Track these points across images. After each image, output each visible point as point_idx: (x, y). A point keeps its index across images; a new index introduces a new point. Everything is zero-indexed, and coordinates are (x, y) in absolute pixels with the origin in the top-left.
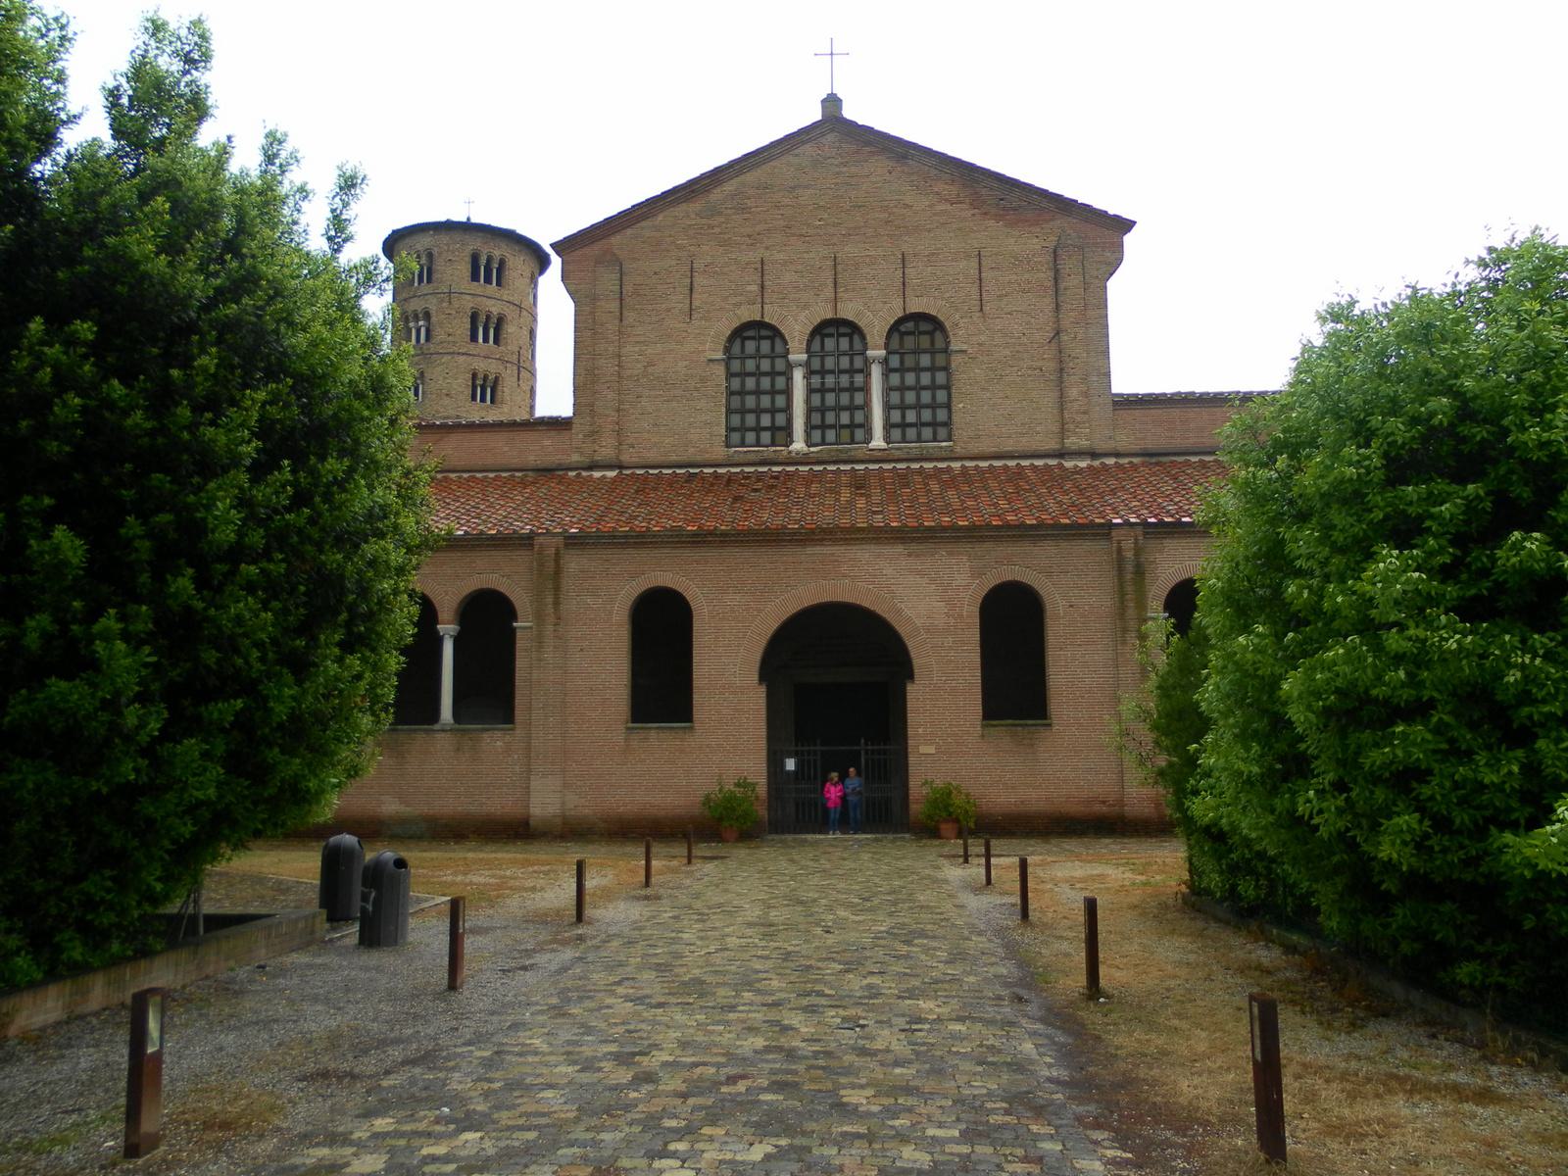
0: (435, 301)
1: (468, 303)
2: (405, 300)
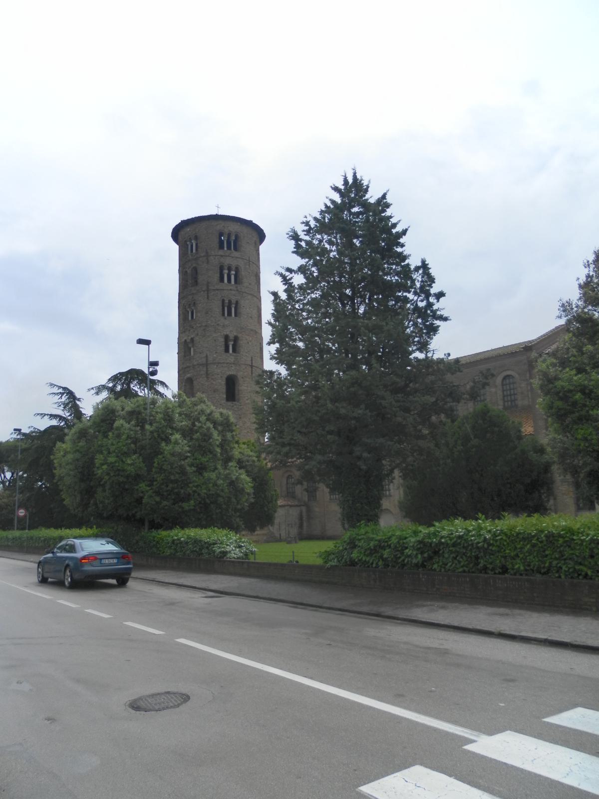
2: (222, 256)
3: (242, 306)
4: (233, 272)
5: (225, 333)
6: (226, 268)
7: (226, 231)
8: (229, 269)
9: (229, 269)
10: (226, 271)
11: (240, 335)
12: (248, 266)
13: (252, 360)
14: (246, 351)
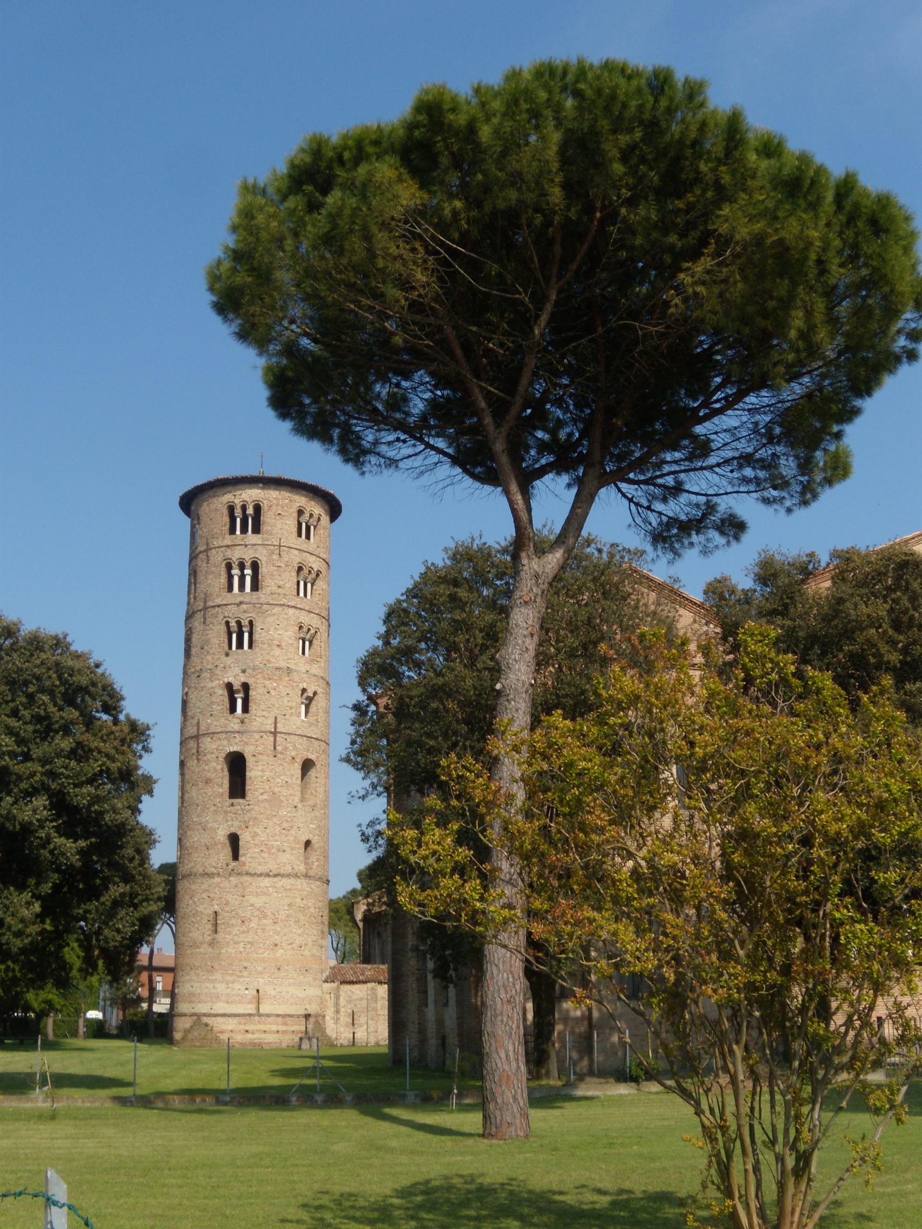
0: (265, 552)
1: (295, 558)
2: (228, 546)
3: (258, 630)
4: (248, 572)
5: (226, 680)
6: (248, 564)
7: (238, 502)
8: (242, 566)
9: (242, 566)
10: (236, 572)
11: (250, 681)
12: (275, 557)
13: (276, 723)
14: (263, 707)
